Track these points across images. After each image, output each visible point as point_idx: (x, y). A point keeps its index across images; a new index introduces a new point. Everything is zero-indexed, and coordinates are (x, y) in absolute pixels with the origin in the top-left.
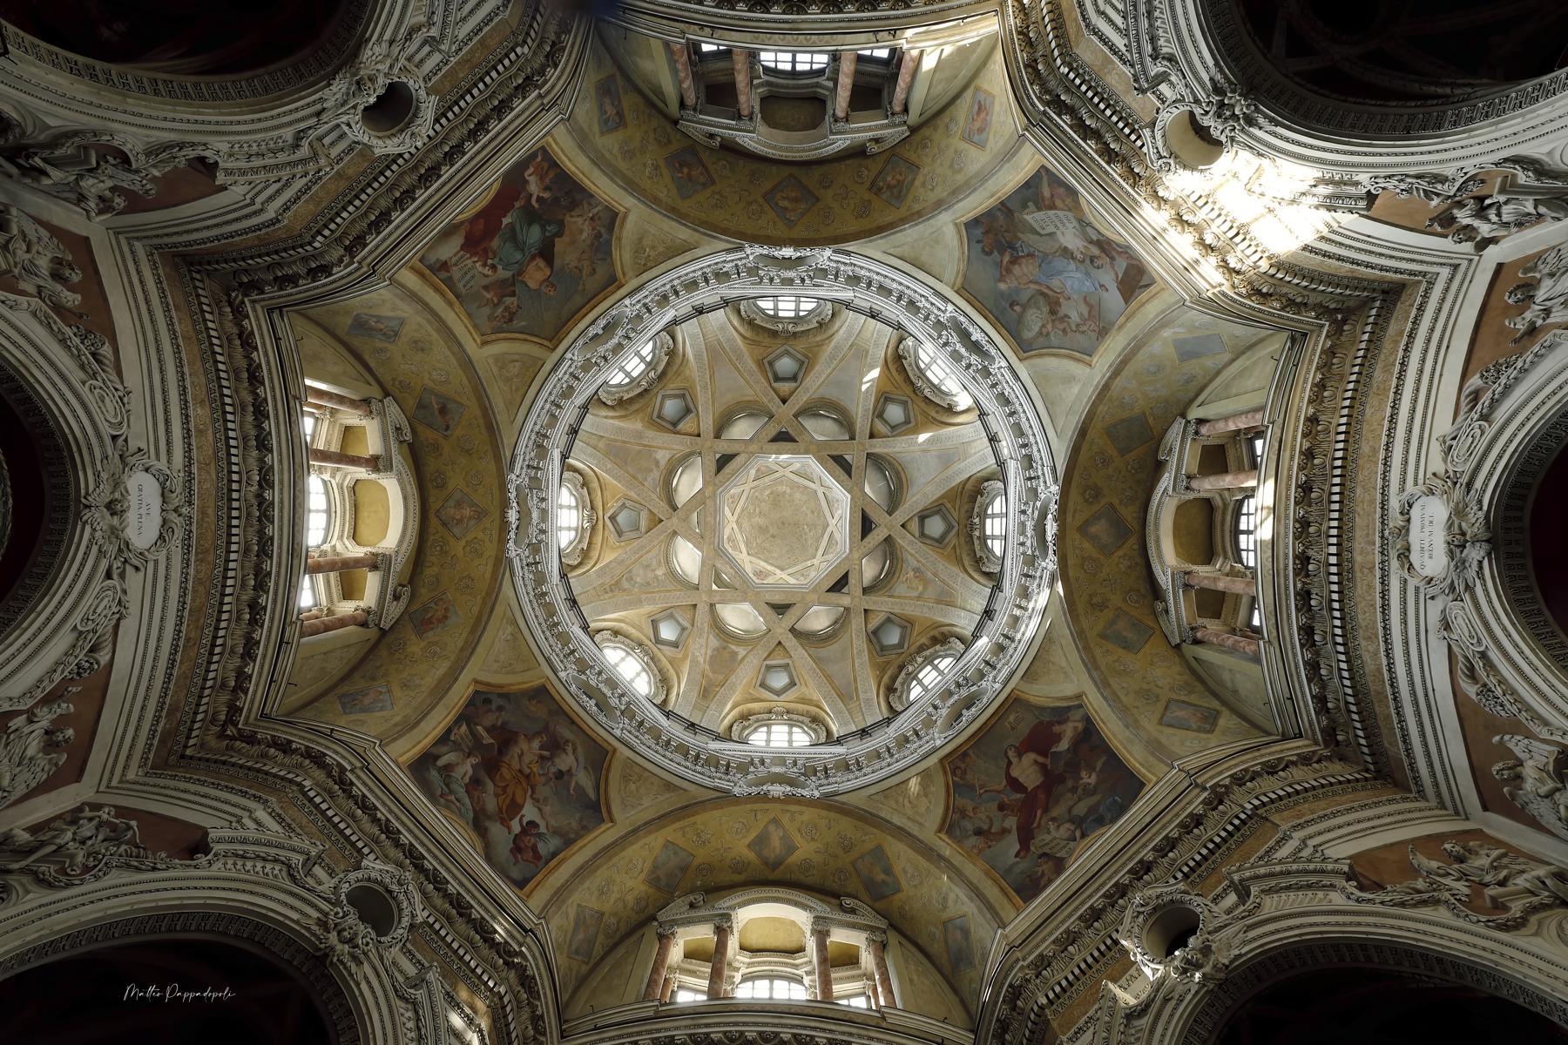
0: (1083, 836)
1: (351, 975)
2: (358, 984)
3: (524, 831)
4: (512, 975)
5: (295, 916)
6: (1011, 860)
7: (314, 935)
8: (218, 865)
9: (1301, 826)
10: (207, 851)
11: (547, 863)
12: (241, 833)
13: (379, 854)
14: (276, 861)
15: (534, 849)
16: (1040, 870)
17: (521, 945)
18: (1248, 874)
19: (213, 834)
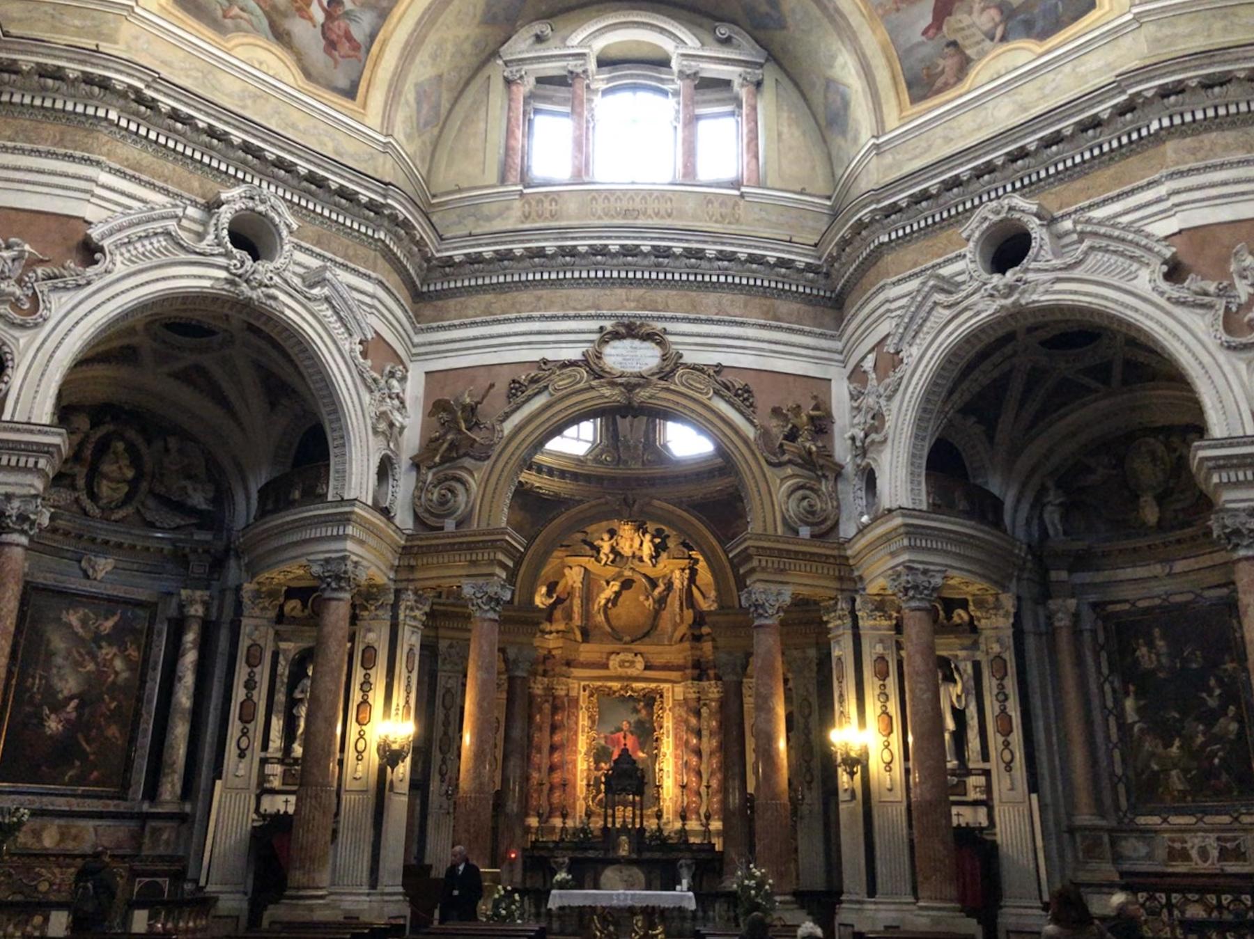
0: (1004, 39)
2: (283, 313)
3: (329, 16)
5: (207, 283)
6: (918, 37)
8: (118, 259)
9: (1182, 174)
11: (368, 51)
12: (113, 224)
13: (219, 156)
14: (156, 234)
15: (348, 37)
16: (941, 62)
17: (385, 197)
18: (1089, 229)
19: (95, 233)
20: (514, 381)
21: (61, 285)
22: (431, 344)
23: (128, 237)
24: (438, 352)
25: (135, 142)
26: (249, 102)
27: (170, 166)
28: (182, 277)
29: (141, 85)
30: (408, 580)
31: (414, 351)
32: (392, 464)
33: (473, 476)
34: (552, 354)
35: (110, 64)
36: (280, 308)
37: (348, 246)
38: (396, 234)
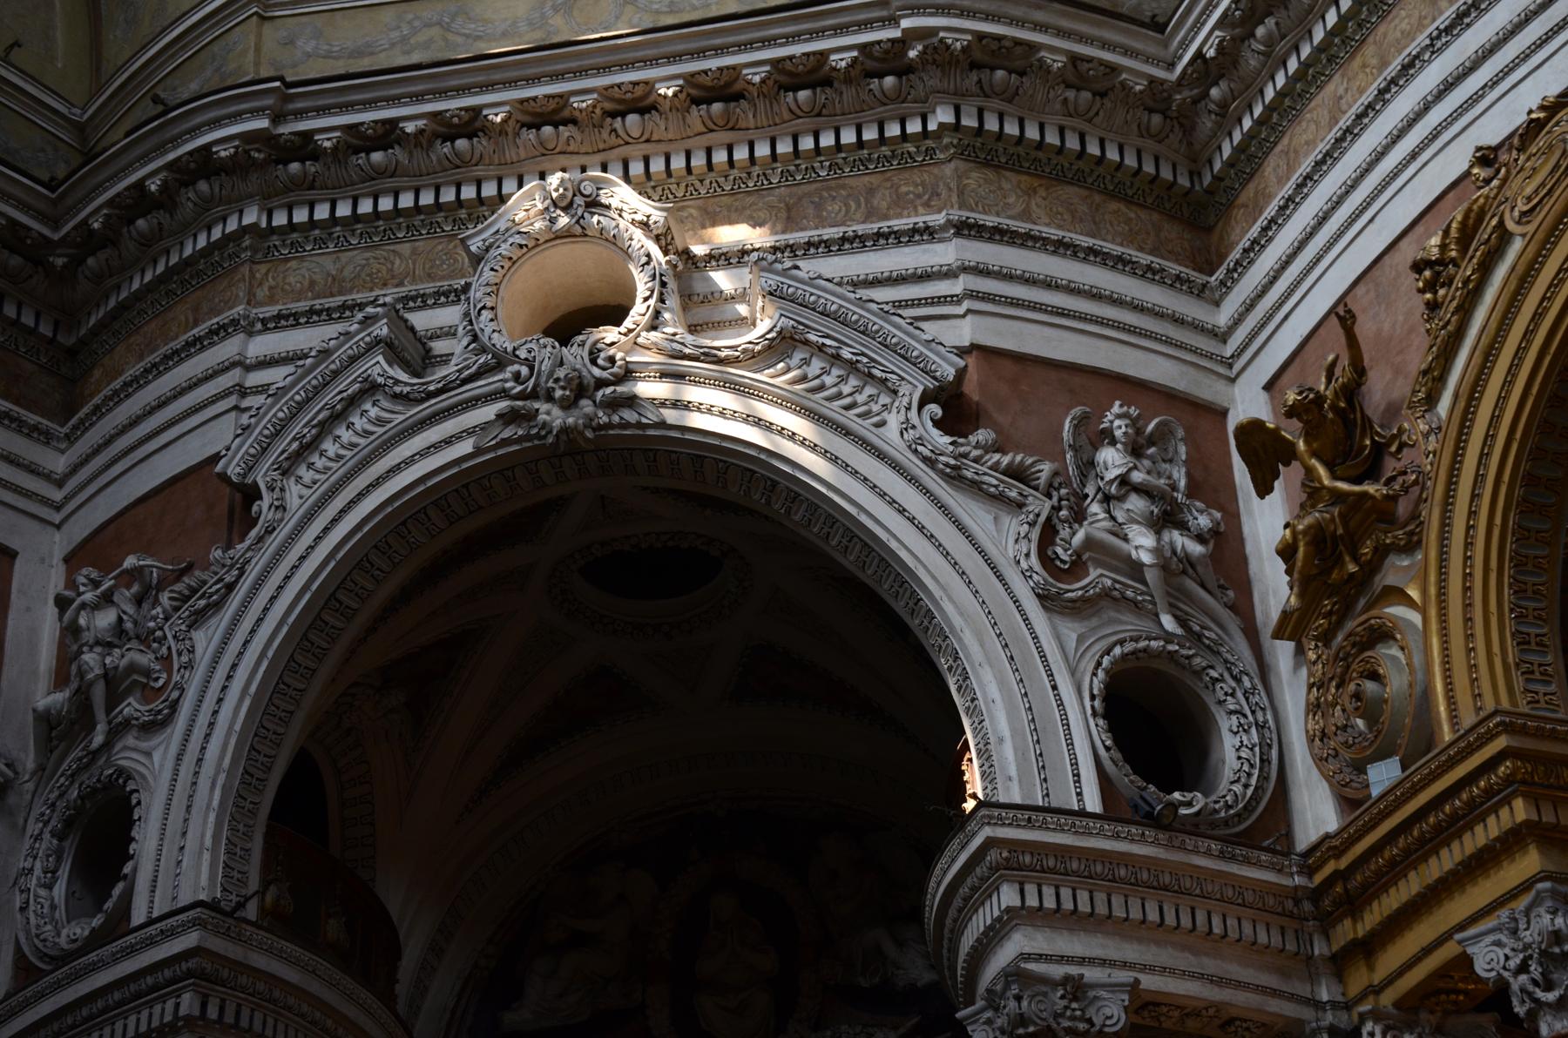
1: (639, 425)
2: (662, 424)
4: (933, 79)
5: (466, 447)
7: (520, 440)
10: (252, 494)
12: (262, 428)
17: (893, 21)
20: (1418, 267)
21: (203, 602)
22: (1250, 306)
23: (294, 439)
24: (1269, 317)
25: (321, 243)
26: (557, 21)
27: (405, 248)
28: (409, 462)
29: (263, 123)
30: (1376, 990)
31: (1228, 351)
32: (1199, 673)
33: (1410, 602)
34: (1495, 126)
35: (199, 120)
36: (651, 416)
37: (871, 191)
38: (985, 91)
